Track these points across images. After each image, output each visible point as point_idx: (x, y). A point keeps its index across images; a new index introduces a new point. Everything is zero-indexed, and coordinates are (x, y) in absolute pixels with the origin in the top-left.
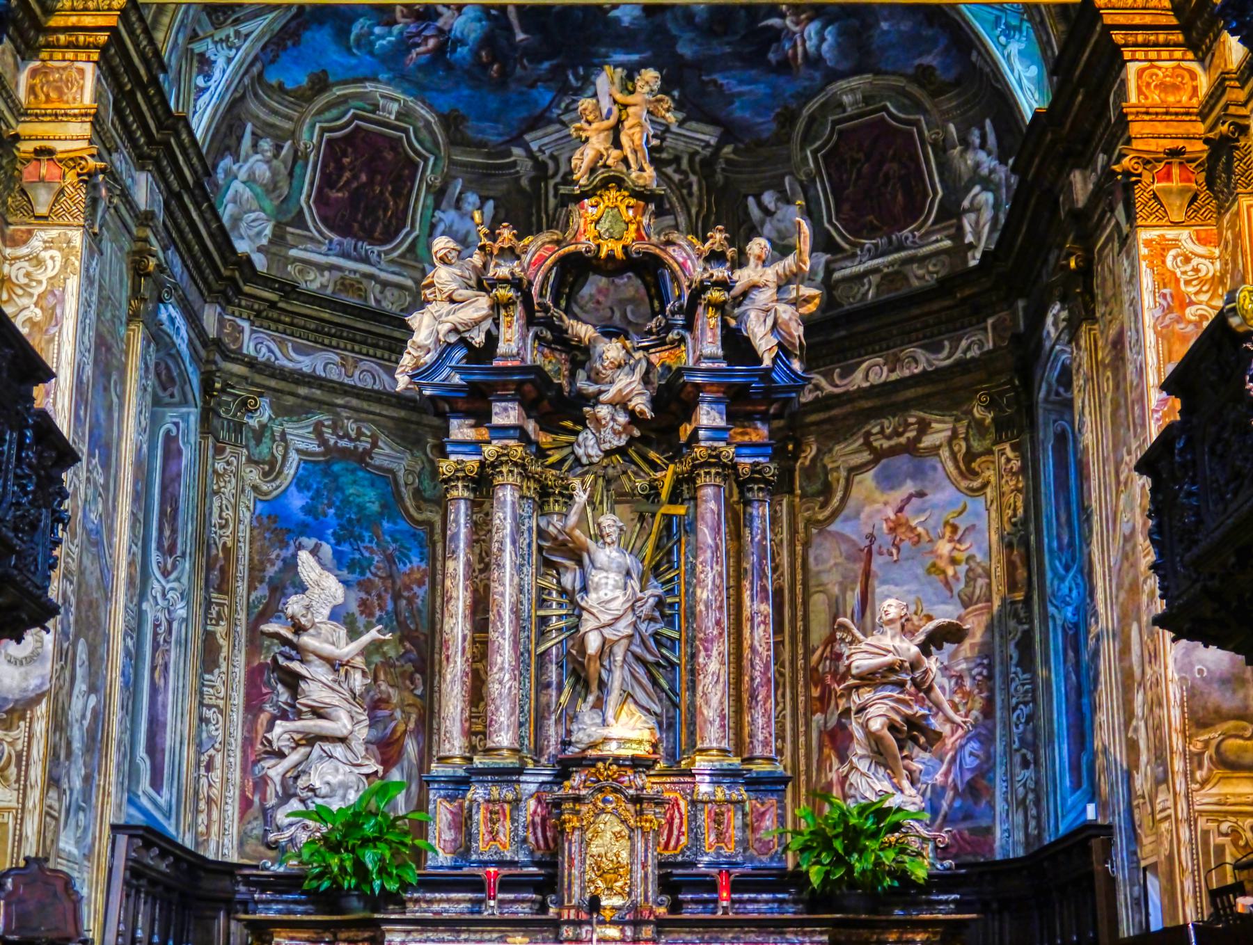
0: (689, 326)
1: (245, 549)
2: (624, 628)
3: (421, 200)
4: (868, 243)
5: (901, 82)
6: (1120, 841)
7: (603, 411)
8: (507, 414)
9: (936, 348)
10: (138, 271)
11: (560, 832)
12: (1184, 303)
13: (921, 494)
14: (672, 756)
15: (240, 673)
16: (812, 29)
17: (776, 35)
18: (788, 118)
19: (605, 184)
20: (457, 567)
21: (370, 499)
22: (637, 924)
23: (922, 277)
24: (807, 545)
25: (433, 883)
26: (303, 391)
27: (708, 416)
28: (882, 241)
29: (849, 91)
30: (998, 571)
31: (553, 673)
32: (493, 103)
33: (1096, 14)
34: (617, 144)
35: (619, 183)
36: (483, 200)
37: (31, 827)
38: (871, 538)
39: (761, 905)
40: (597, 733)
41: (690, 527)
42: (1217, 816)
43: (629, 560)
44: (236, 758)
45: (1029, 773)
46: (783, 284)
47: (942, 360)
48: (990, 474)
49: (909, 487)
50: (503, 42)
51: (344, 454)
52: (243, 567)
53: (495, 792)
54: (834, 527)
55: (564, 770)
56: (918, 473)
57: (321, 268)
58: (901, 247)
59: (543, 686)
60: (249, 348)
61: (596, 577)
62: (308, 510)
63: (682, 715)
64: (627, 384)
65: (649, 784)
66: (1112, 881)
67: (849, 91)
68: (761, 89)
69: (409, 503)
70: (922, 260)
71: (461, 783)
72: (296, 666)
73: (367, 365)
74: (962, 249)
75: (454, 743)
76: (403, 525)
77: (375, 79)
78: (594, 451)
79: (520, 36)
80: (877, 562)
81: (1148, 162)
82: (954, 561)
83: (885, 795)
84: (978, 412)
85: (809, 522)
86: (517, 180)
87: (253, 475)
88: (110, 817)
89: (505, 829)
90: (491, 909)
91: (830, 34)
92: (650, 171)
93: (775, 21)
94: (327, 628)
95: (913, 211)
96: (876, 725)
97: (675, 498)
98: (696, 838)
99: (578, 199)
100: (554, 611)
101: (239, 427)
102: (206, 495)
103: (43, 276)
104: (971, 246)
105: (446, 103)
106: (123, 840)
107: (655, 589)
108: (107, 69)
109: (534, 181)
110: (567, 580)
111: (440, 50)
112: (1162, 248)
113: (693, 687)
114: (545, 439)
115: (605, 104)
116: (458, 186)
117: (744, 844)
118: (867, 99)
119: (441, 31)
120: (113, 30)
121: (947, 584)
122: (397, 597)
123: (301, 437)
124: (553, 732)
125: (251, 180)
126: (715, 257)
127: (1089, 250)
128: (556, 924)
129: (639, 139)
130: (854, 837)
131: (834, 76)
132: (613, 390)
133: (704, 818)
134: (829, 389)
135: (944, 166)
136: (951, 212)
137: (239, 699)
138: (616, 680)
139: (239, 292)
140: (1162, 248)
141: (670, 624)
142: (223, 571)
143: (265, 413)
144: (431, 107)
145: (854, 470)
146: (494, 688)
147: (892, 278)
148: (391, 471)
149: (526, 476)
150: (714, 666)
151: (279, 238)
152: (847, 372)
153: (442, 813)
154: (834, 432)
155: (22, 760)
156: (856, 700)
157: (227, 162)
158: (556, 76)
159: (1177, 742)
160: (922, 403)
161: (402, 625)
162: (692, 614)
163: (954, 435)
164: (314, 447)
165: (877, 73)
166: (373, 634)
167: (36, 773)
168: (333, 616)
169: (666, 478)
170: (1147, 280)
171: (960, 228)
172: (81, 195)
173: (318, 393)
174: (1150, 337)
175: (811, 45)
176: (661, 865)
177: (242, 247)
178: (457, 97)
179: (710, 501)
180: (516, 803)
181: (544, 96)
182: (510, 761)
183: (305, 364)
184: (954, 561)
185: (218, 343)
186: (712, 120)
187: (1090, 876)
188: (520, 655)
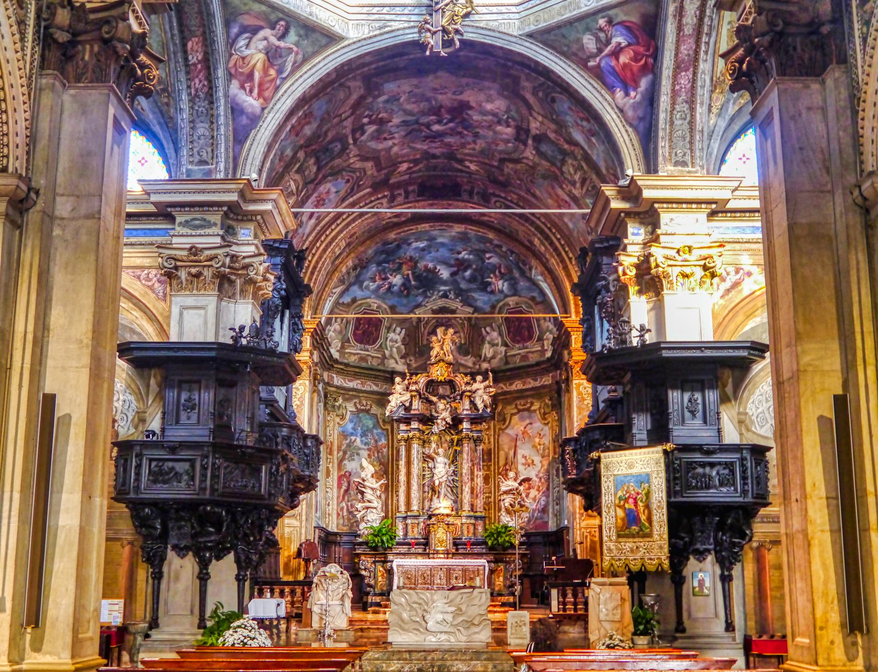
0: (461, 399)
1: (336, 441)
2: (444, 478)
3: (383, 331)
4: (517, 346)
5: (526, 300)
6: (571, 531)
7: (439, 421)
8: (415, 425)
9: (536, 380)
10: (315, 379)
11: (429, 532)
12: (584, 399)
13: (531, 424)
14: (457, 510)
15: (336, 478)
16: (500, 283)
17: (490, 284)
18: (493, 307)
19: (439, 361)
20: (402, 463)
21: (370, 423)
22: (448, 554)
23: (533, 359)
24: (499, 436)
25: (398, 544)
26: (351, 393)
27: (465, 425)
28: (521, 345)
29: (512, 301)
30: (551, 448)
31: (426, 489)
32: (405, 301)
33: (564, 325)
34: (442, 349)
35: (443, 361)
36: (402, 329)
37: (303, 531)
38: (517, 435)
39: (477, 549)
40: (439, 505)
41: (461, 452)
42: (586, 528)
43: (446, 460)
44: (335, 502)
45: (557, 507)
46: (485, 388)
47: (537, 384)
48: (550, 419)
49: (528, 421)
50: (408, 285)
51: (363, 411)
52: (335, 447)
53: (413, 521)
54: (507, 431)
55: (430, 517)
56: (530, 417)
57: (355, 354)
58: (527, 348)
59: (424, 492)
60: (336, 383)
61: (437, 465)
62: (354, 429)
63: (459, 499)
64: (446, 415)
65: (451, 520)
66: (568, 541)
67: (512, 301)
68: (485, 298)
69: (381, 424)
70: (532, 352)
71: (405, 518)
72: (363, 489)
73: (369, 383)
74: (543, 351)
75: (402, 508)
76: (380, 431)
77: (370, 298)
78: (437, 431)
79: (413, 283)
80: (519, 443)
81: (576, 363)
82: (540, 444)
83: (508, 521)
84: (547, 401)
85: (500, 429)
86: (412, 323)
87: (338, 420)
88: (314, 525)
89: (416, 530)
90: (413, 550)
91: (506, 284)
92: (451, 357)
93: (489, 280)
94: (371, 479)
95: (530, 337)
96: (507, 504)
97: (457, 445)
98: (462, 533)
99: (432, 364)
100: (427, 473)
101: (334, 406)
102: (326, 429)
103: (299, 393)
104: (546, 350)
105: (390, 303)
106: (317, 530)
107: (453, 468)
108: (312, 336)
109: (417, 323)
110: (430, 465)
111: (389, 288)
112: (579, 385)
113: (462, 494)
114: (424, 428)
115: (439, 338)
116: (394, 326)
117: (474, 534)
118: (517, 304)
119: (390, 283)
120: (315, 329)
121: (538, 451)
122: (378, 452)
123: (350, 407)
124: (427, 504)
125: (335, 331)
126: (467, 384)
127: (568, 373)
128: (428, 554)
129: (449, 349)
130: (499, 534)
131: (506, 296)
132: (442, 416)
133: (465, 527)
134: (505, 389)
135: (539, 326)
136: (540, 339)
137: (336, 485)
138: (443, 491)
139: (333, 366)
140: (579, 385)
141: (456, 475)
142: (331, 449)
143: (341, 400)
144: (386, 304)
145: (512, 415)
146: (413, 495)
147: (524, 357)
148: (376, 415)
149: (420, 439)
150: (467, 489)
151: (343, 347)
152: (511, 384)
153: (400, 526)
154: (507, 402)
155: (300, 515)
156: (502, 498)
157: (329, 327)
158: (424, 292)
159: (578, 510)
160: (532, 396)
161: (380, 460)
162: (461, 475)
163: (540, 408)
164: (354, 409)
165: (520, 296)
166: (382, 481)
167: (304, 518)
168: (372, 476)
169: (456, 438)
170: (575, 394)
171: (543, 344)
172: (308, 372)
173: (355, 393)
174: (575, 409)
175: (500, 287)
176: (454, 539)
177: (333, 351)
178: (393, 301)
179: (466, 448)
180: (418, 524)
181: (420, 299)
182: (417, 514)
183: (351, 385)
184: (540, 444)
185: (328, 384)
186: (470, 305)
187: (563, 539)
188: (419, 485)
